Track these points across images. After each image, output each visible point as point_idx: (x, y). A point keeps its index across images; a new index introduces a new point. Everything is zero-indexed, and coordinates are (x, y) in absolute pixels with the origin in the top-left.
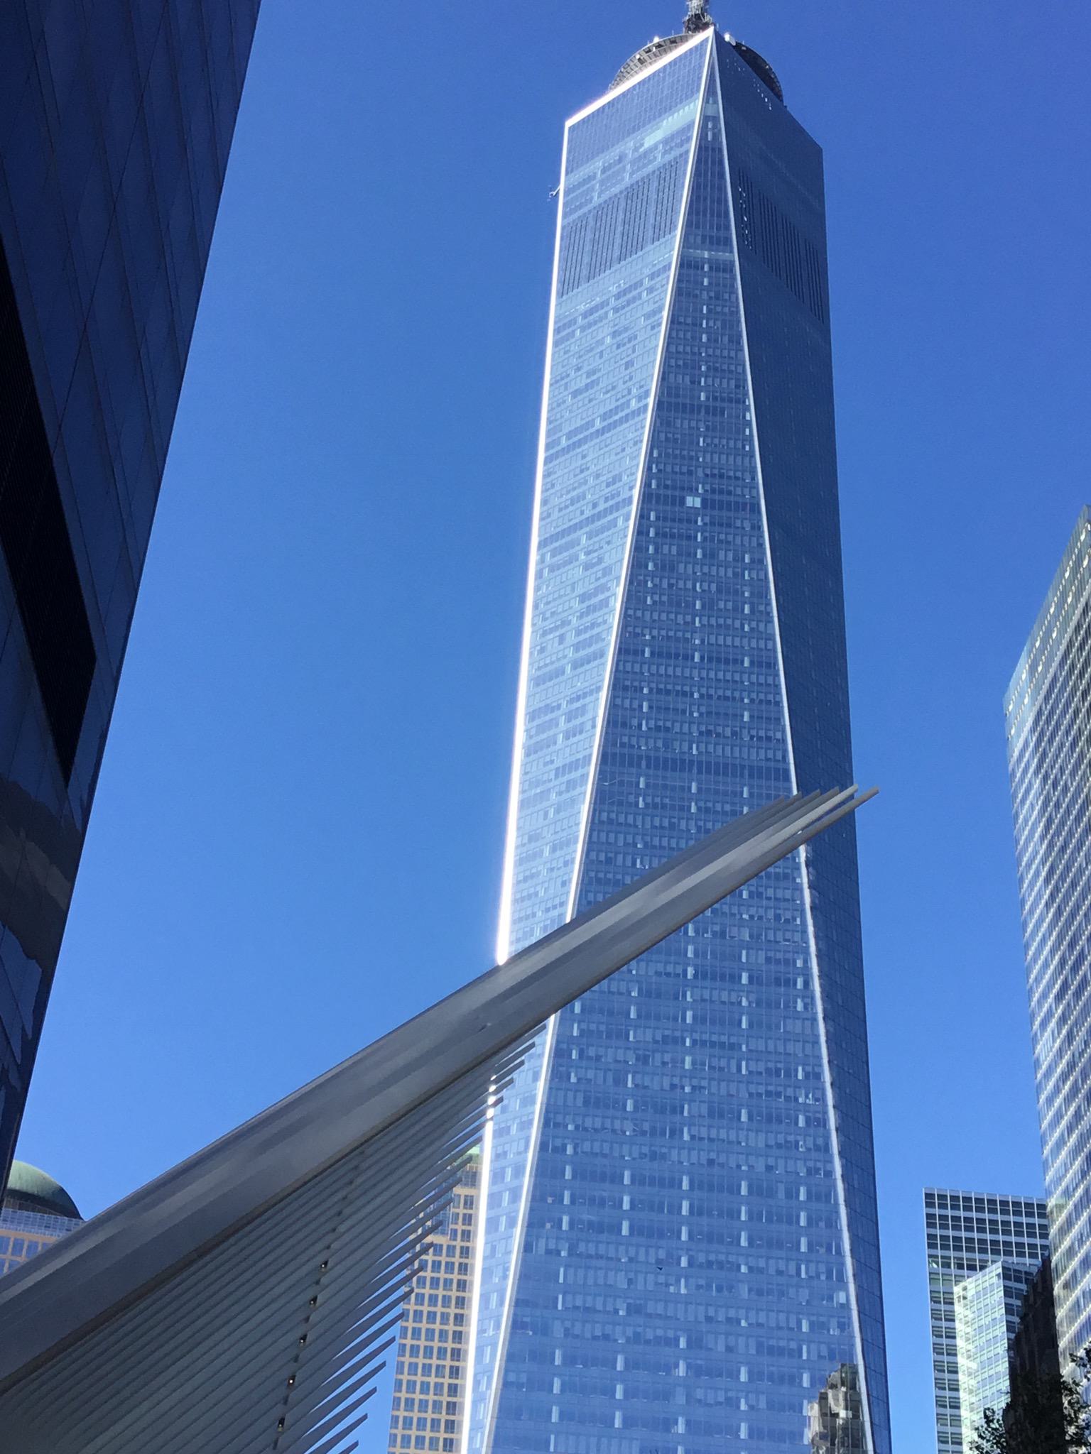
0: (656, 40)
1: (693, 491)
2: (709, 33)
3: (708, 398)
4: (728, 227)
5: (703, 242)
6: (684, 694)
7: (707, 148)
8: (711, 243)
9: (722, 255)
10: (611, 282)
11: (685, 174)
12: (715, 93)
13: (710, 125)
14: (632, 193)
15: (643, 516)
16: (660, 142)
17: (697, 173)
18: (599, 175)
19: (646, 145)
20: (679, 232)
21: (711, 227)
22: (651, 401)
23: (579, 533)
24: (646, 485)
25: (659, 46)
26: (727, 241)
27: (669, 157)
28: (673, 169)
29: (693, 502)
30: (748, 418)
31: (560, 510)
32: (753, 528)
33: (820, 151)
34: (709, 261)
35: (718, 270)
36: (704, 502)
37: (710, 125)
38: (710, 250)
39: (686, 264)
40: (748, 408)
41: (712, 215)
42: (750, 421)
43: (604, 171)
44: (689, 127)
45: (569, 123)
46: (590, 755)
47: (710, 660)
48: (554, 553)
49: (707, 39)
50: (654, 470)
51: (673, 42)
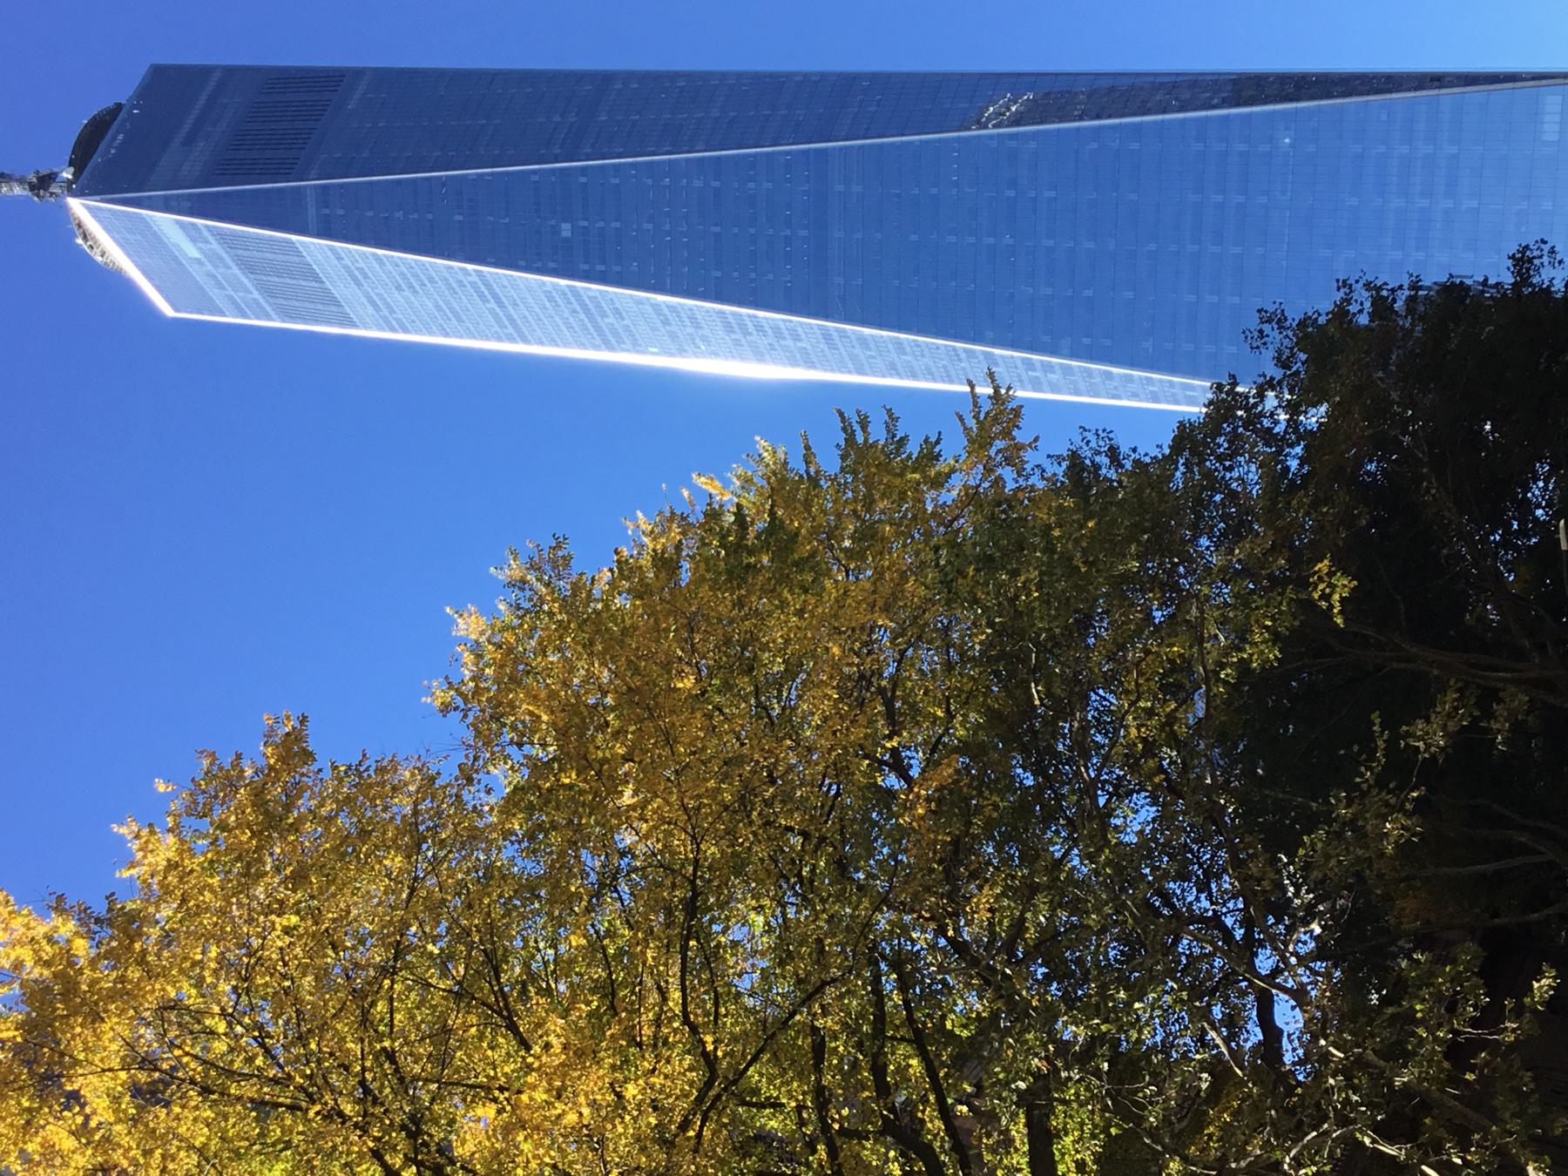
0: (80, 241)
1: (556, 231)
10: (342, 290)
14: (249, 267)
20: (294, 237)
22: (470, 267)
23: (602, 324)
25: (85, 238)
27: (211, 239)
28: (221, 236)
29: (566, 230)
36: (565, 220)
39: (326, 232)
44: (177, 222)
45: (168, 311)
50: (539, 264)
51: (80, 226)
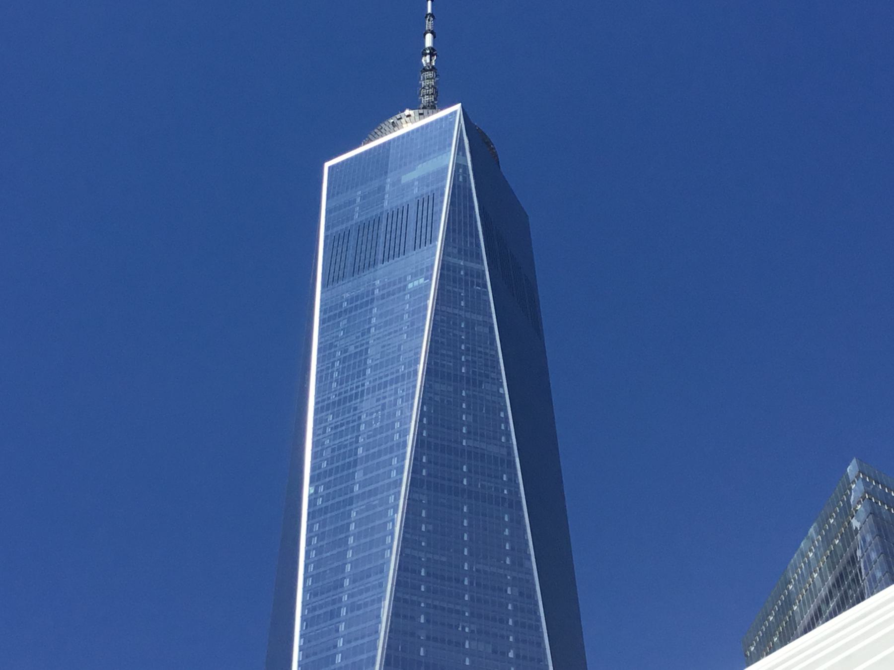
2: (458, 107)
3: (467, 372)
6: (457, 612)
7: (459, 186)
8: (466, 254)
11: (442, 202)
13: (461, 171)
15: (416, 459)
16: (418, 179)
17: (452, 203)
18: (358, 200)
22: (421, 368)
24: (419, 434)
25: (409, 116)
30: (501, 391)
31: (333, 450)
32: (510, 479)
34: (466, 268)
35: (472, 276)
37: (461, 171)
38: (466, 260)
40: (502, 386)
41: (466, 236)
43: (363, 198)
45: (327, 165)
46: (375, 657)
47: (478, 585)
48: (327, 487)
49: (455, 112)
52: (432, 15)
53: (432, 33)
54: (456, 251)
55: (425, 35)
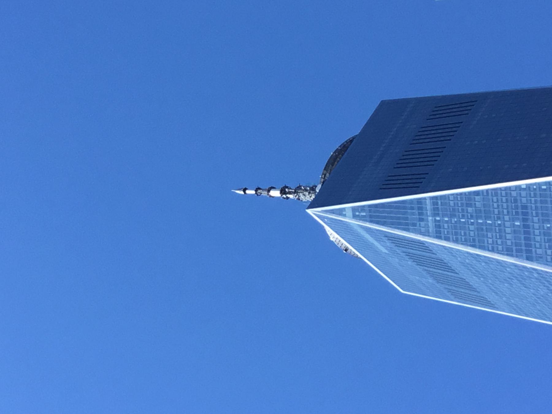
3: (518, 219)
4: (411, 201)
5: (421, 220)
9: (429, 206)
12: (339, 209)
19: (386, 251)
21: (413, 214)
26: (419, 201)
30: (524, 187)
33: (383, 103)
34: (435, 215)
41: (405, 213)
42: (526, 185)
52: (256, 191)
53: (269, 191)
54: (423, 224)
55: (273, 197)
